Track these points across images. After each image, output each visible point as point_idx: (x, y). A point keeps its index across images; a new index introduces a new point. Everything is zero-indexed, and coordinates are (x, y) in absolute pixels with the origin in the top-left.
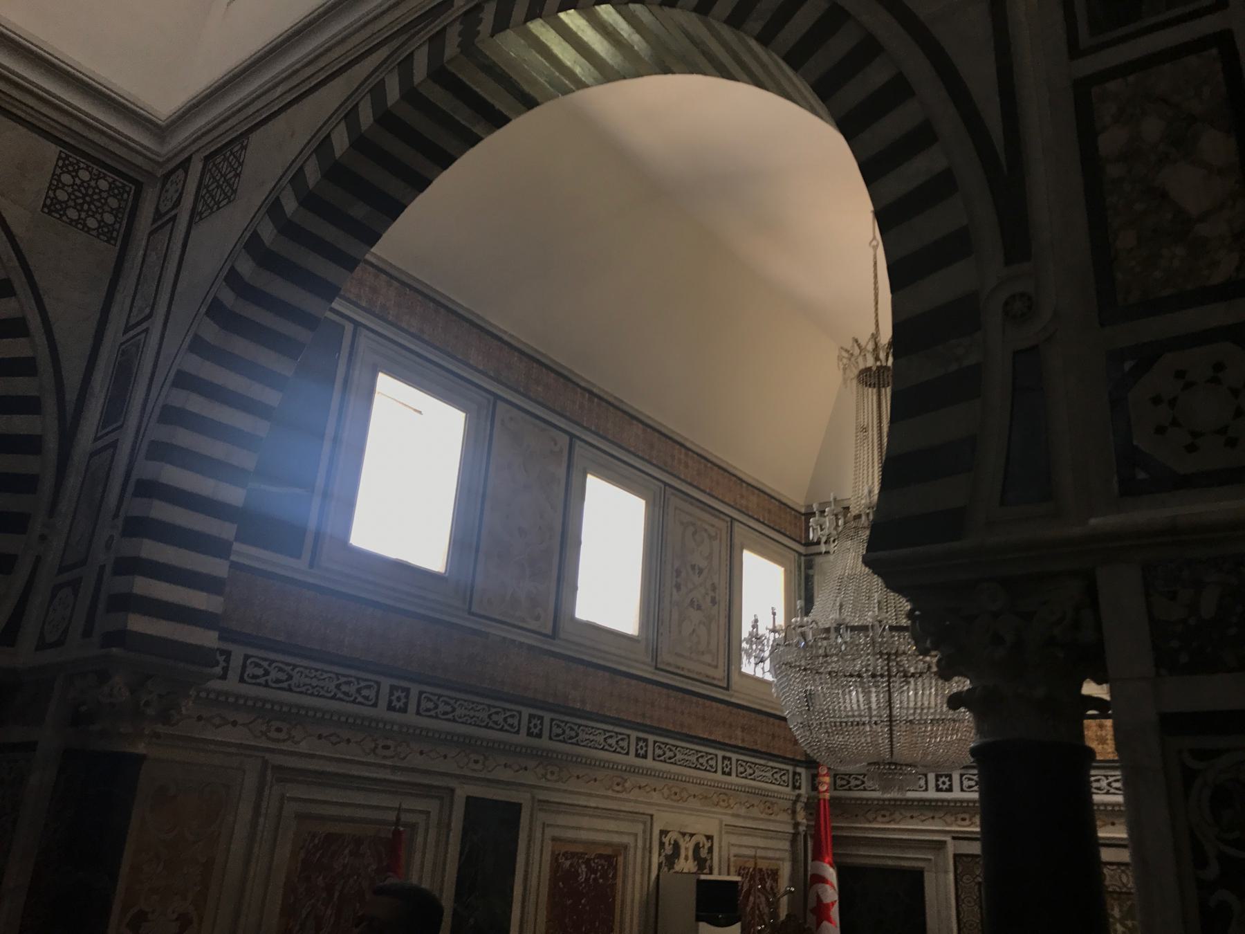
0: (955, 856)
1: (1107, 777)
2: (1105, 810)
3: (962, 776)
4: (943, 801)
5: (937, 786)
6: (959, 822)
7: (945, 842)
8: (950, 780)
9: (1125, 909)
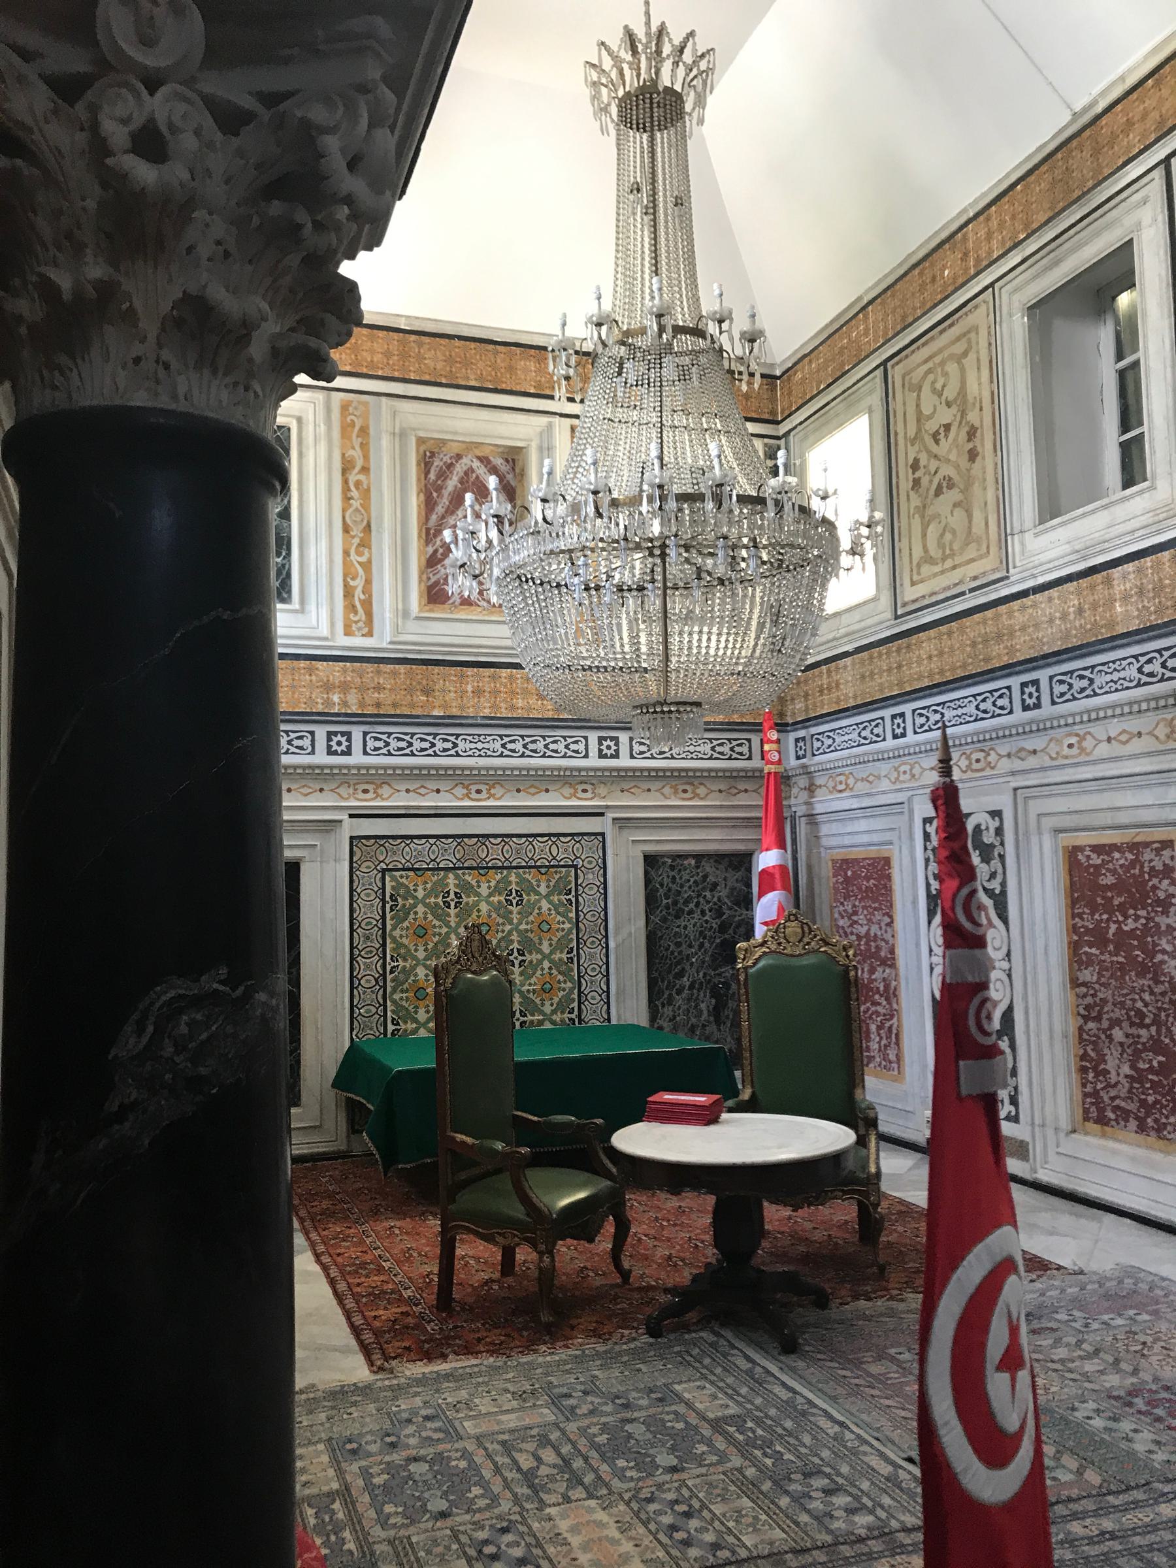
0: (351, 838)
1: (543, 737)
2: (438, 774)
3: (365, 734)
4: (340, 767)
5: (329, 747)
6: (361, 796)
7: (341, 821)
8: (349, 740)
9: (552, 884)
